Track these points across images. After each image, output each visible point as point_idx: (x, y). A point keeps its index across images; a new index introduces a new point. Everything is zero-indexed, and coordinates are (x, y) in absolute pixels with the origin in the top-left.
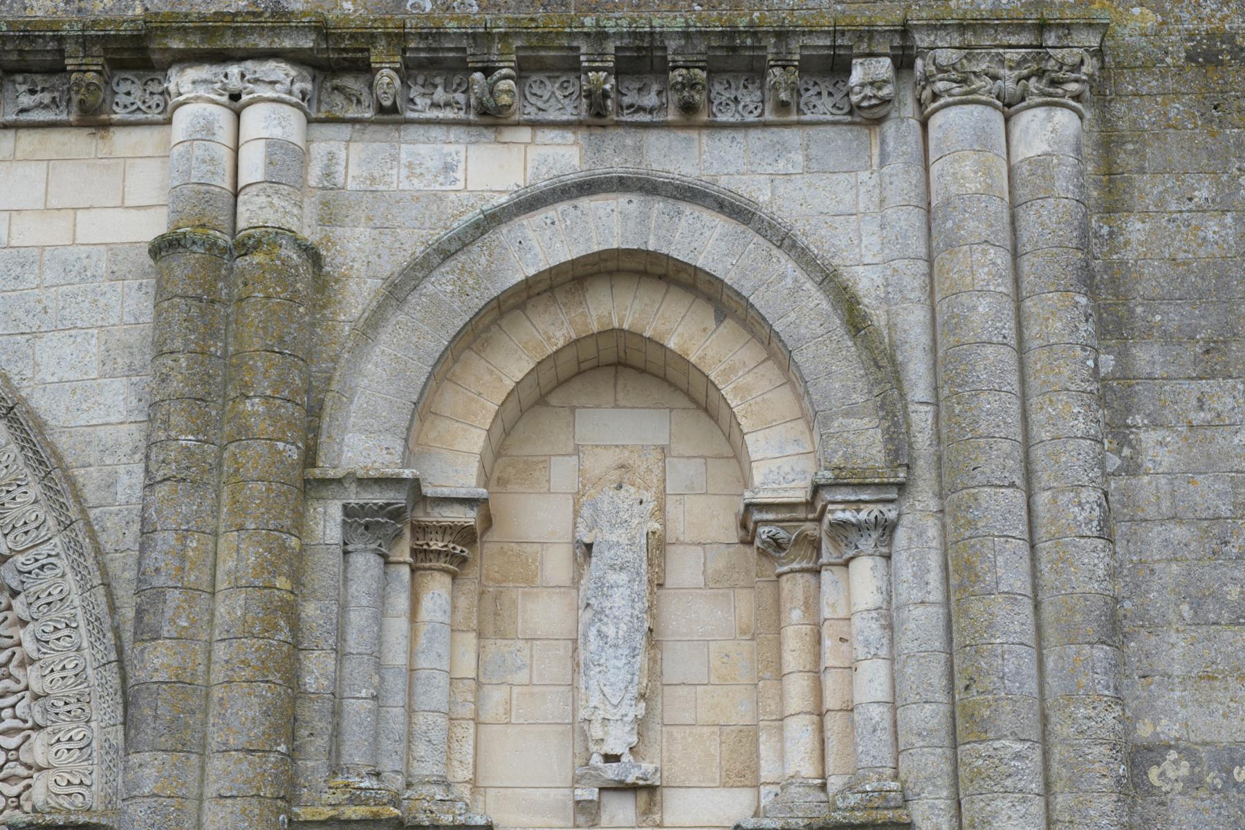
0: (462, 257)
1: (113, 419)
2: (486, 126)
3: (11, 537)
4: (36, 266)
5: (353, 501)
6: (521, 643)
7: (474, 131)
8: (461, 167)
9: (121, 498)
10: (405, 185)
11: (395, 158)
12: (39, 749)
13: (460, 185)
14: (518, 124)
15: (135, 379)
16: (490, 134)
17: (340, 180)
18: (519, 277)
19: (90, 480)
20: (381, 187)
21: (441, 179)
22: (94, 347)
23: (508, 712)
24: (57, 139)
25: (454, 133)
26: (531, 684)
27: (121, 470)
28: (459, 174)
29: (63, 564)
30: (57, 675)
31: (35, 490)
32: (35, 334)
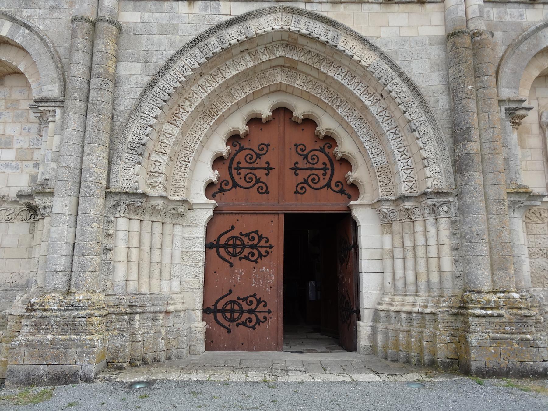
0: (529, 40)
1: (436, 84)
2: (531, 4)
3: (412, 116)
4: (408, 42)
5: (508, 107)
6: (528, 150)
7: (527, 5)
8: (525, 15)
9: (441, 105)
10: (510, 20)
11: (506, 12)
12: (427, 172)
13: (525, 20)
14: (539, 3)
15: (441, 73)
16: (531, 6)
17: (492, 18)
18: (545, 46)
19: (431, 100)
20: (503, 20)
21: (520, 18)
22: (428, 65)
23: (526, 167)
24: (410, 6)
25: (521, 5)
26: (532, 160)
27: (440, 98)
28: (525, 17)
29: (427, 123)
30: (430, 153)
31: (416, 103)
32: (410, 61)
